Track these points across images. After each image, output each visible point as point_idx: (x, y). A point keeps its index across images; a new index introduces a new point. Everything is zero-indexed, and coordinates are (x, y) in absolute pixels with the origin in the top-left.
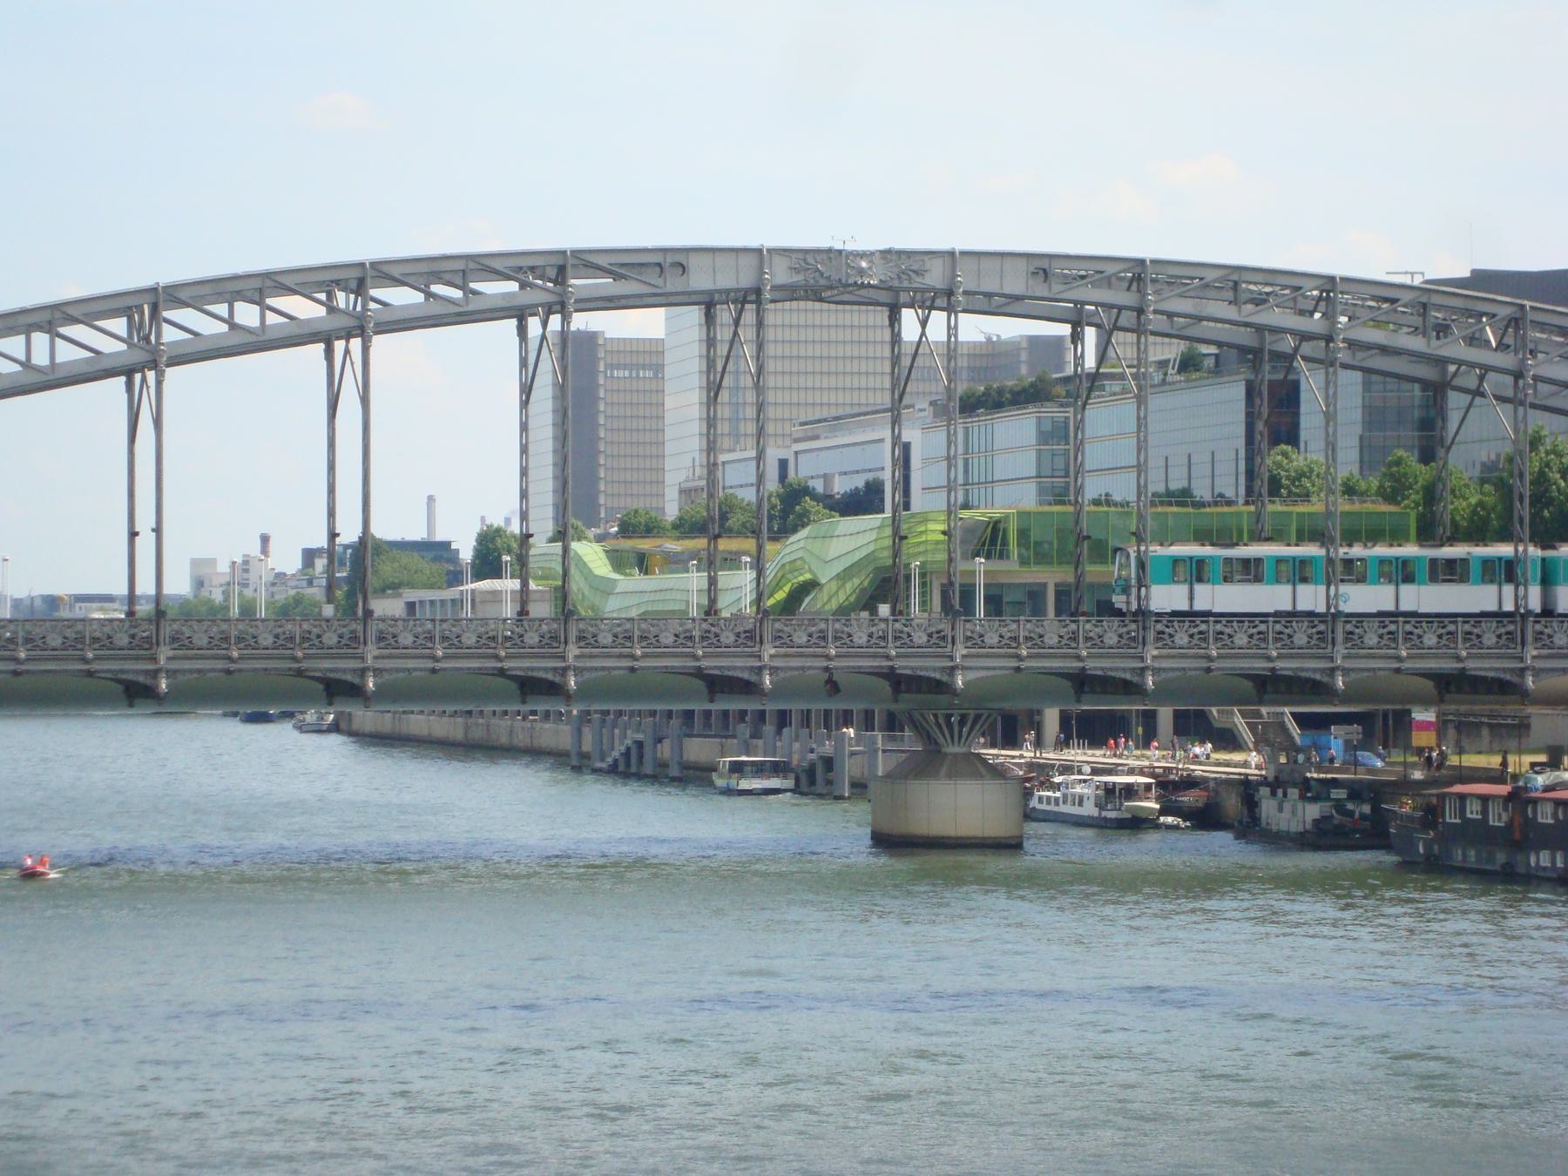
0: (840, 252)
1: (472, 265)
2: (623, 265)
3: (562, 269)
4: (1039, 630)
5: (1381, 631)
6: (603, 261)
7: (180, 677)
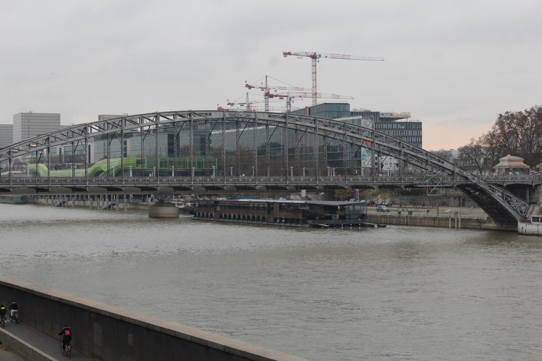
0: (237, 111)
1: (175, 114)
2: (200, 114)
3: (190, 115)
4: (291, 178)
5: (324, 178)
6: (197, 113)
7: (127, 188)
